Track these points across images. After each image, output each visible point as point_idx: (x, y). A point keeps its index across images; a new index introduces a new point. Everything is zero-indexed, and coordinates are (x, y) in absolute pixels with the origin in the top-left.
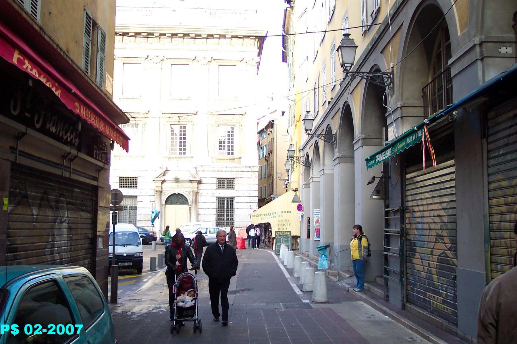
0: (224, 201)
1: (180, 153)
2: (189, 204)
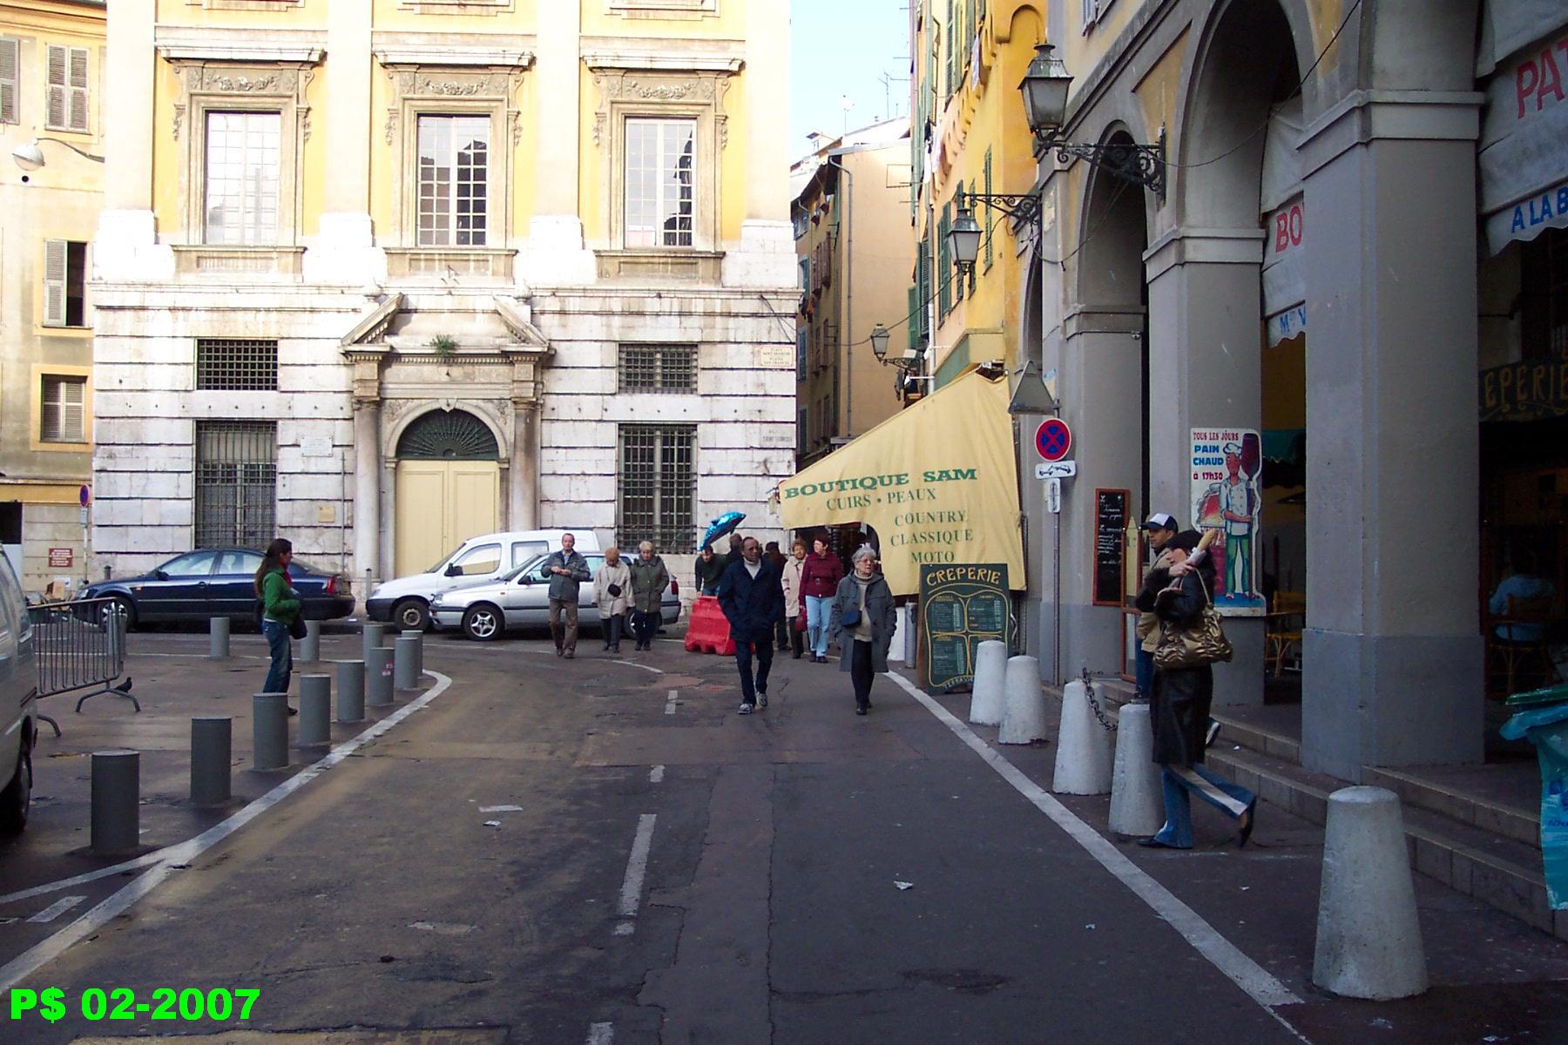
0: (652, 441)
1: (463, 239)
2: (503, 454)
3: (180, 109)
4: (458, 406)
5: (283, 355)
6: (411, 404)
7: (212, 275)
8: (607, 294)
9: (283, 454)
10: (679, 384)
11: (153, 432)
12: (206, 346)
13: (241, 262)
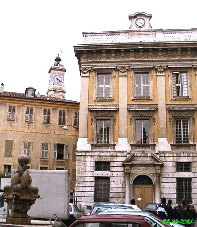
0: (183, 182)
2: (154, 184)
3: (92, 120)
4: (145, 174)
5: (112, 164)
6: (136, 174)
7: (98, 150)
8: (173, 153)
9: (111, 183)
10: (188, 170)
11: (87, 179)
12: (97, 163)
13: (103, 147)
